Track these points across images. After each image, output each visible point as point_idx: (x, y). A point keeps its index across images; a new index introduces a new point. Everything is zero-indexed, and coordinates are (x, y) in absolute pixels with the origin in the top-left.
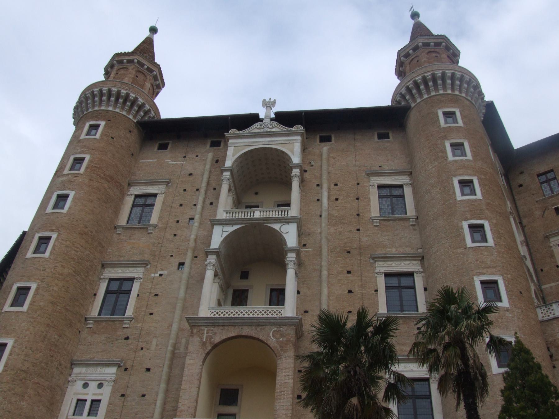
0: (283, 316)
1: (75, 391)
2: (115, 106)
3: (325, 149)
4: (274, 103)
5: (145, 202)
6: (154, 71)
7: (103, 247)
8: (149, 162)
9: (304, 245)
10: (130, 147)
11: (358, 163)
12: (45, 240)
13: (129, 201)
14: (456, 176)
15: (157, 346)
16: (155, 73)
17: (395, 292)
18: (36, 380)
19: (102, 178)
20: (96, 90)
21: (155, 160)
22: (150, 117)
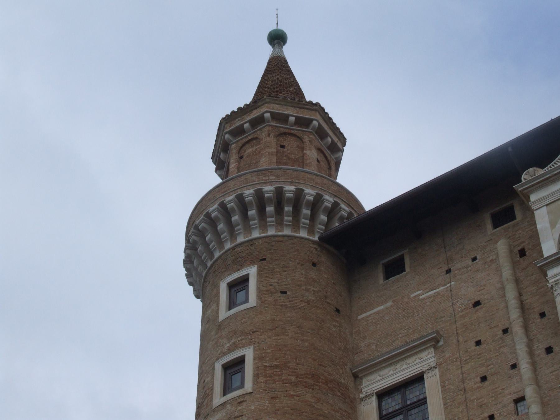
2: (264, 226)
6: (311, 120)
8: (378, 313)
10: (326, 297)
16: (315, 123)
19: (296, 385)
20: (213, 208)
21: (390, 304)
22: (342, 218)
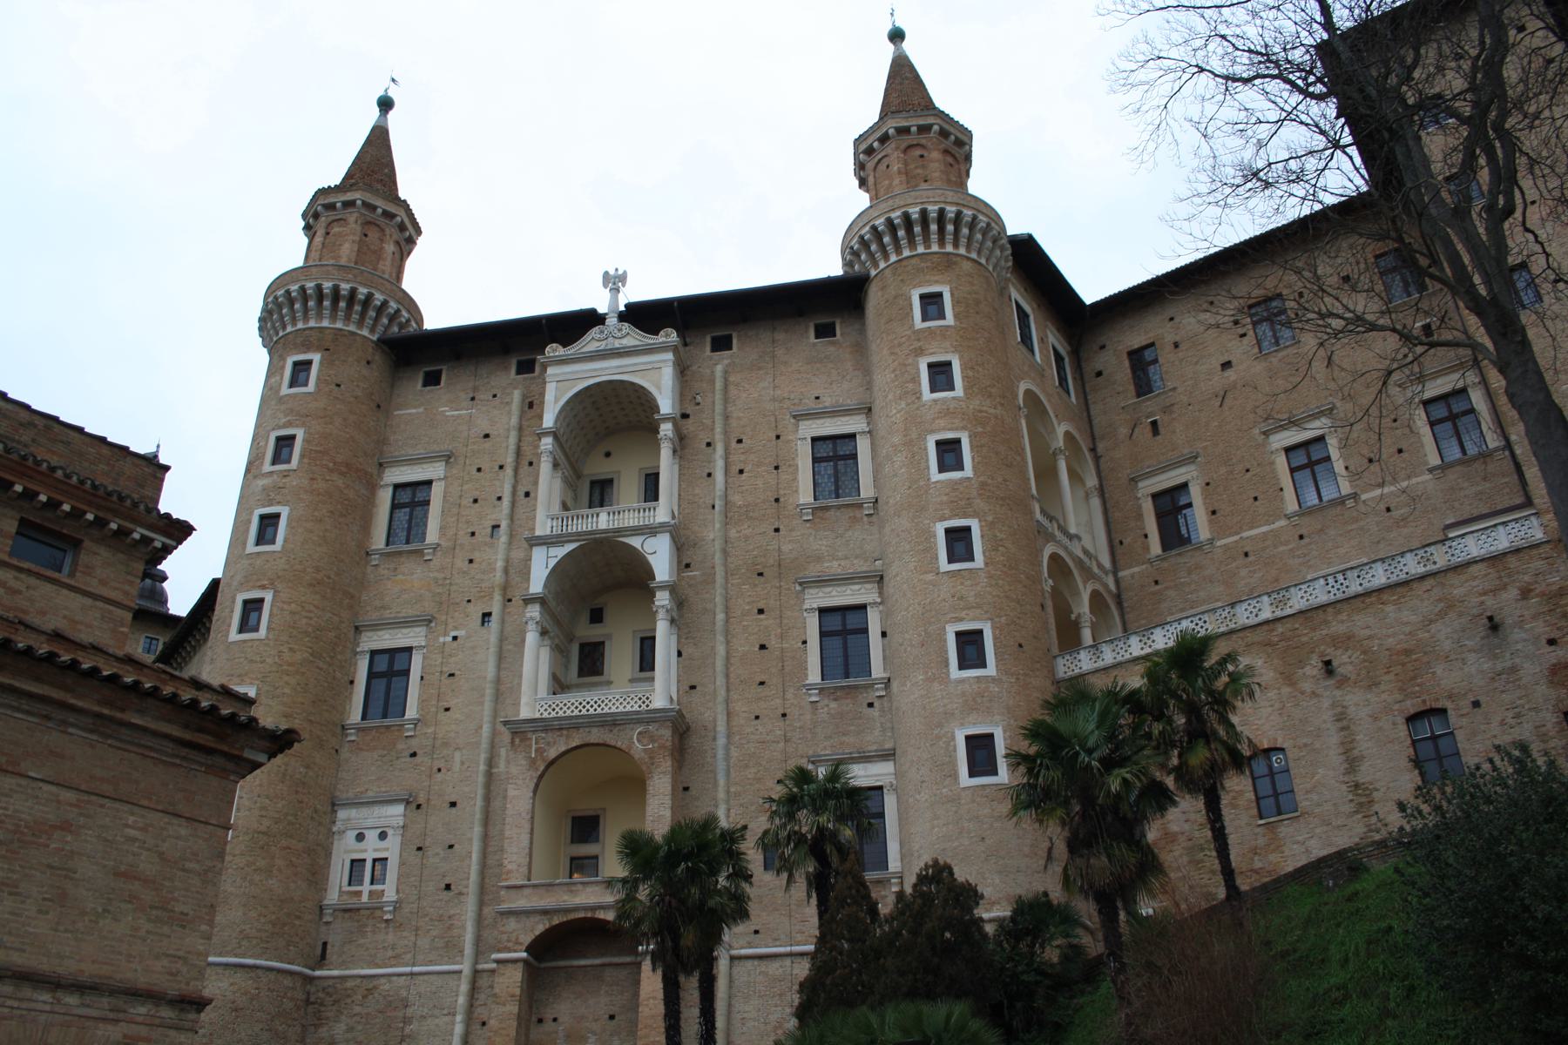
0: (652, 706)
1: (345, 850)
2: (333, 318)
3: (719, 368)
4: (622, 278)
5: (412, 498)
7: (352, 597)
9: (688, 566)
11: (778, 392)
12: (253, 606)
13: (385, 497)
14: (932, 432)
15: (462, 763)
17: (836, 642)
18: (284, 843)
19: (331, 471)
